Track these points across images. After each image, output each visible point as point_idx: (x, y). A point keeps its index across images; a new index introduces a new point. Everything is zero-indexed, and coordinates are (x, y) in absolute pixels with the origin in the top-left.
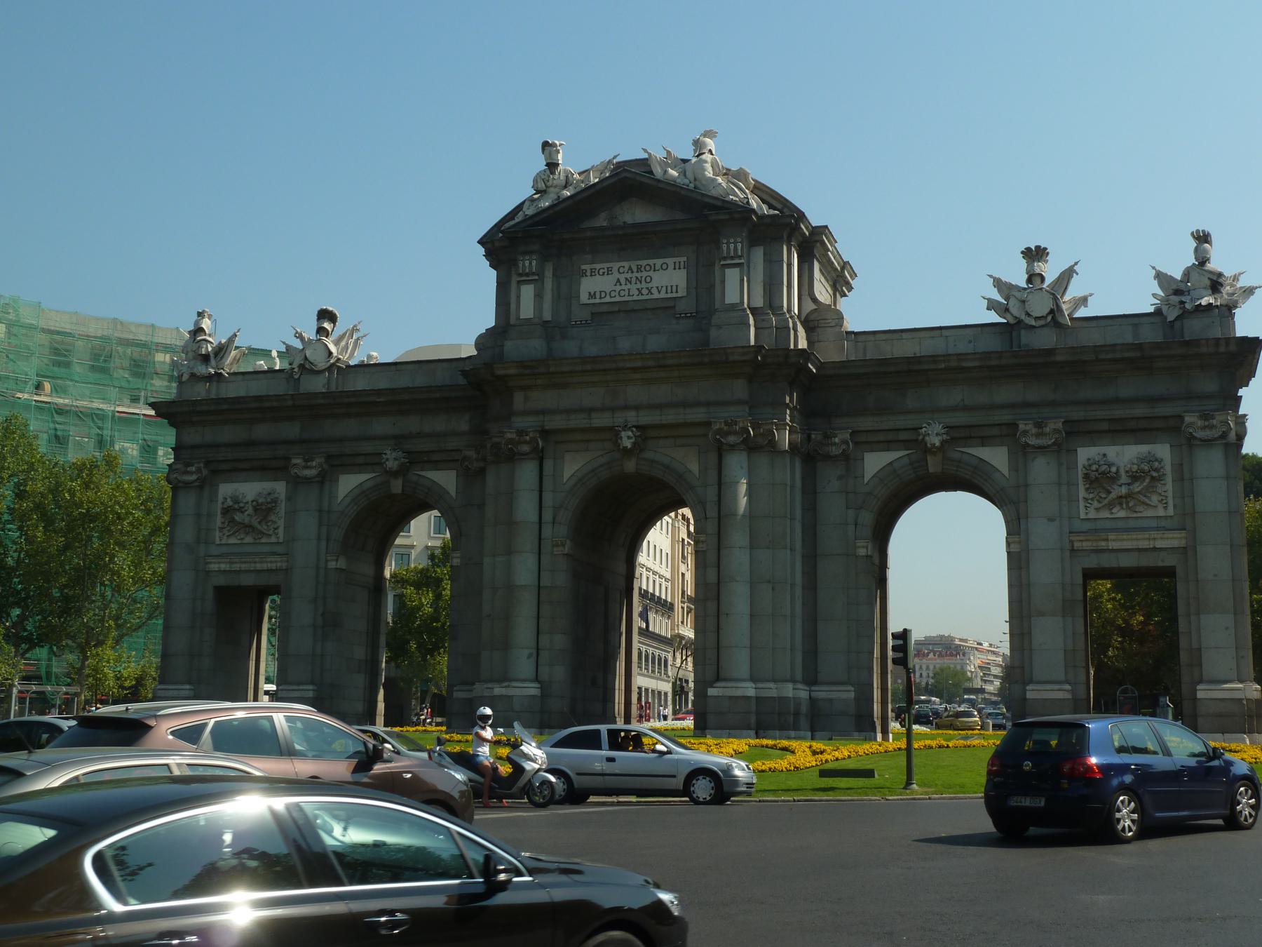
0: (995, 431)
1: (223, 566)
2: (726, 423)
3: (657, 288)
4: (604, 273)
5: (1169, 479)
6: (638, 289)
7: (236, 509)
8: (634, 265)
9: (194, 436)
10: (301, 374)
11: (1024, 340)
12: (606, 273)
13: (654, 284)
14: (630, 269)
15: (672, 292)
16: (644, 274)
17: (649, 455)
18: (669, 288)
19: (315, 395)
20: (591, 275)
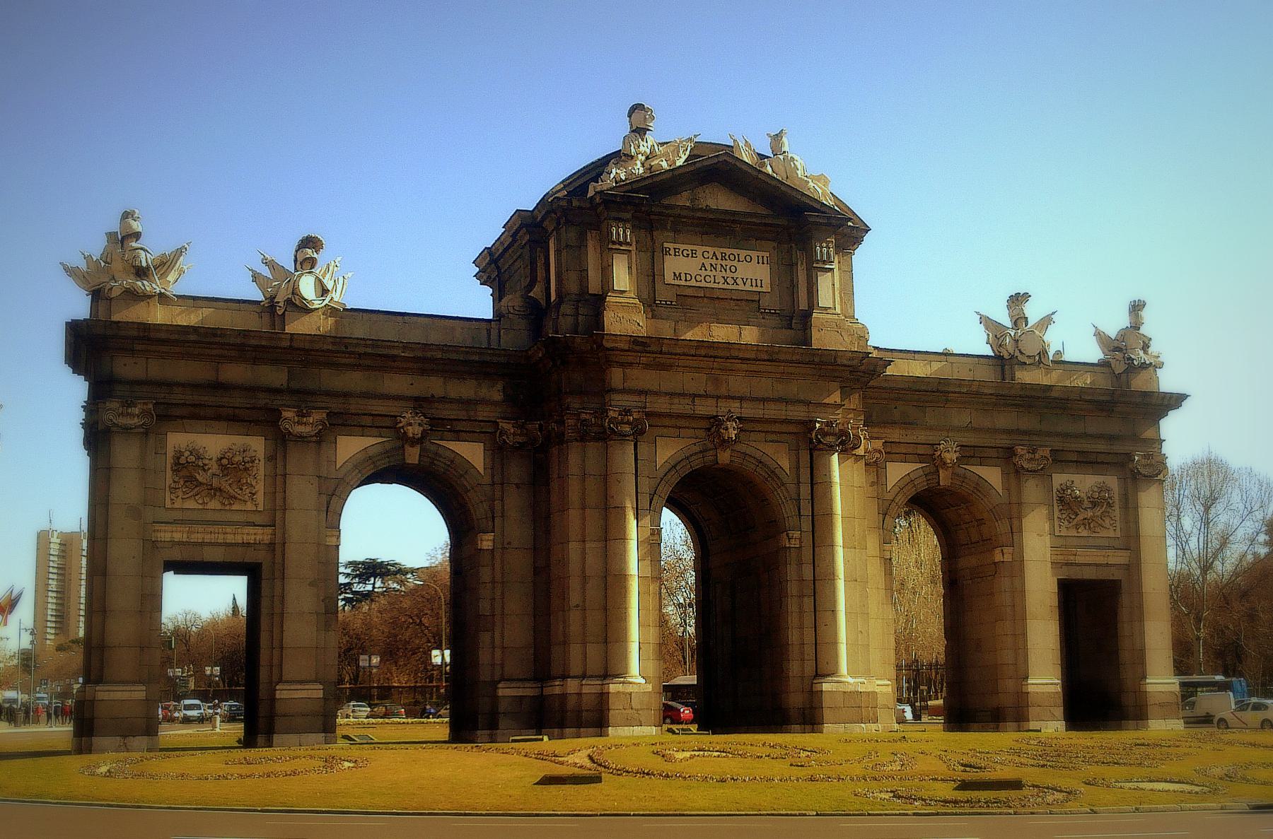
0: (993, 453)
1: (177, 537)
3: (743, 279)
5: (1117, 507)
6: (724, 277)
8: (718, 251)
9: (127, 367)
10: (286, 310)
12: (690, 255)
15: (757, 286)
16: (729, 263)
17: (739, 447)
18: (754, 281)
20: (675, 255)
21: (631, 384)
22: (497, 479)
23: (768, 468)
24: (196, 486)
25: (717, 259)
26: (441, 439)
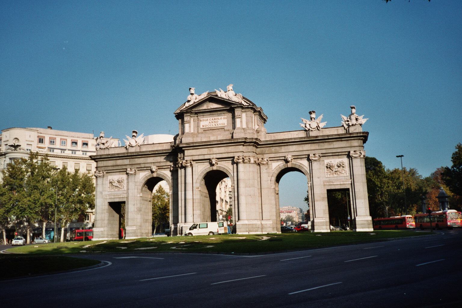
0: (304, 156)
2: (238, 157)
8: (213, 118)
9: (101, 164)
11: (310, 134)
14: (213, 119)
16: (216, 120)
17: (218, 165)
19: (133, 153)
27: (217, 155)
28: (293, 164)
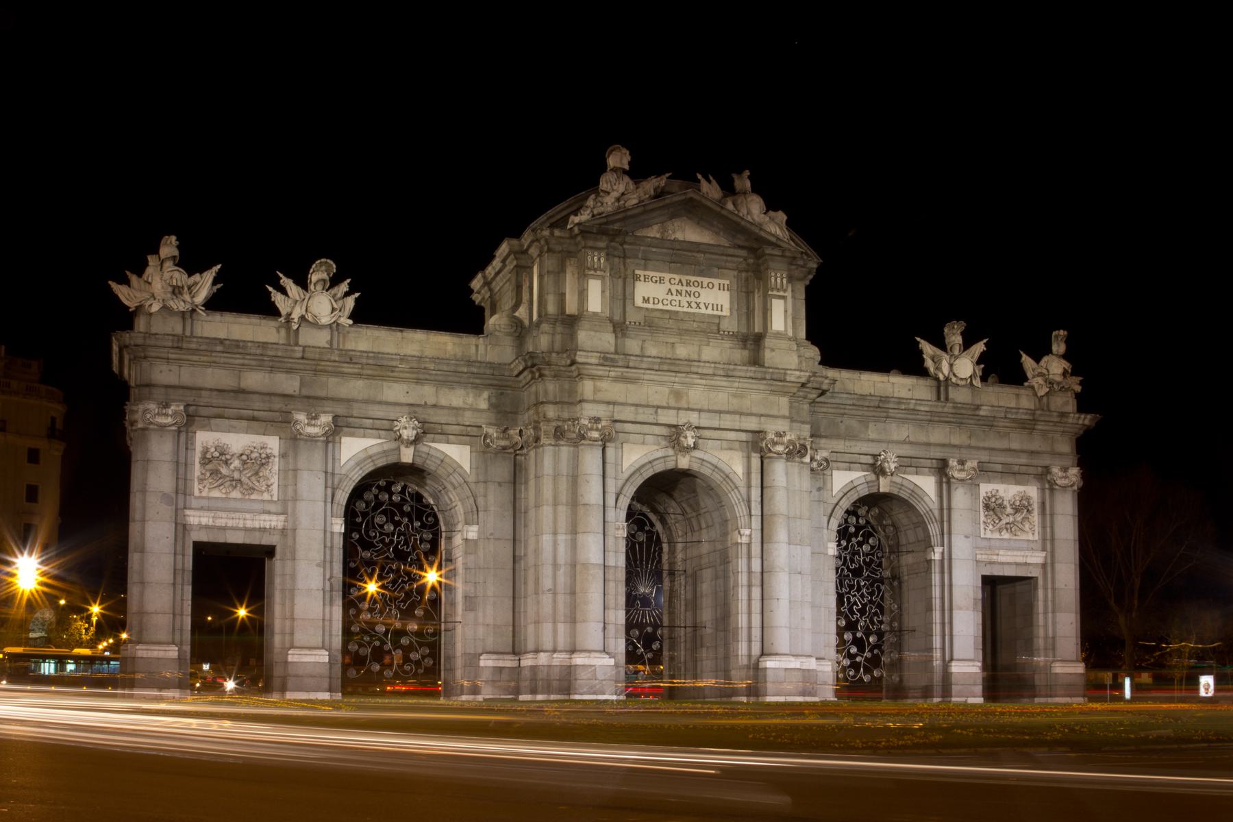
1: (204, 521)
4: (656, 281)
7: (221, 460)
8: (684, 278)
13: (701, 300)
14: (680, 281)
16: (693, 289)
20: (645, 281)
21: (600, 396)
22: (481, 478)
23: (723, 472)
24: (221, 478)
25: (682, 285)
26: (433, 441)
27: (703, 414)
28: (894, 482)
